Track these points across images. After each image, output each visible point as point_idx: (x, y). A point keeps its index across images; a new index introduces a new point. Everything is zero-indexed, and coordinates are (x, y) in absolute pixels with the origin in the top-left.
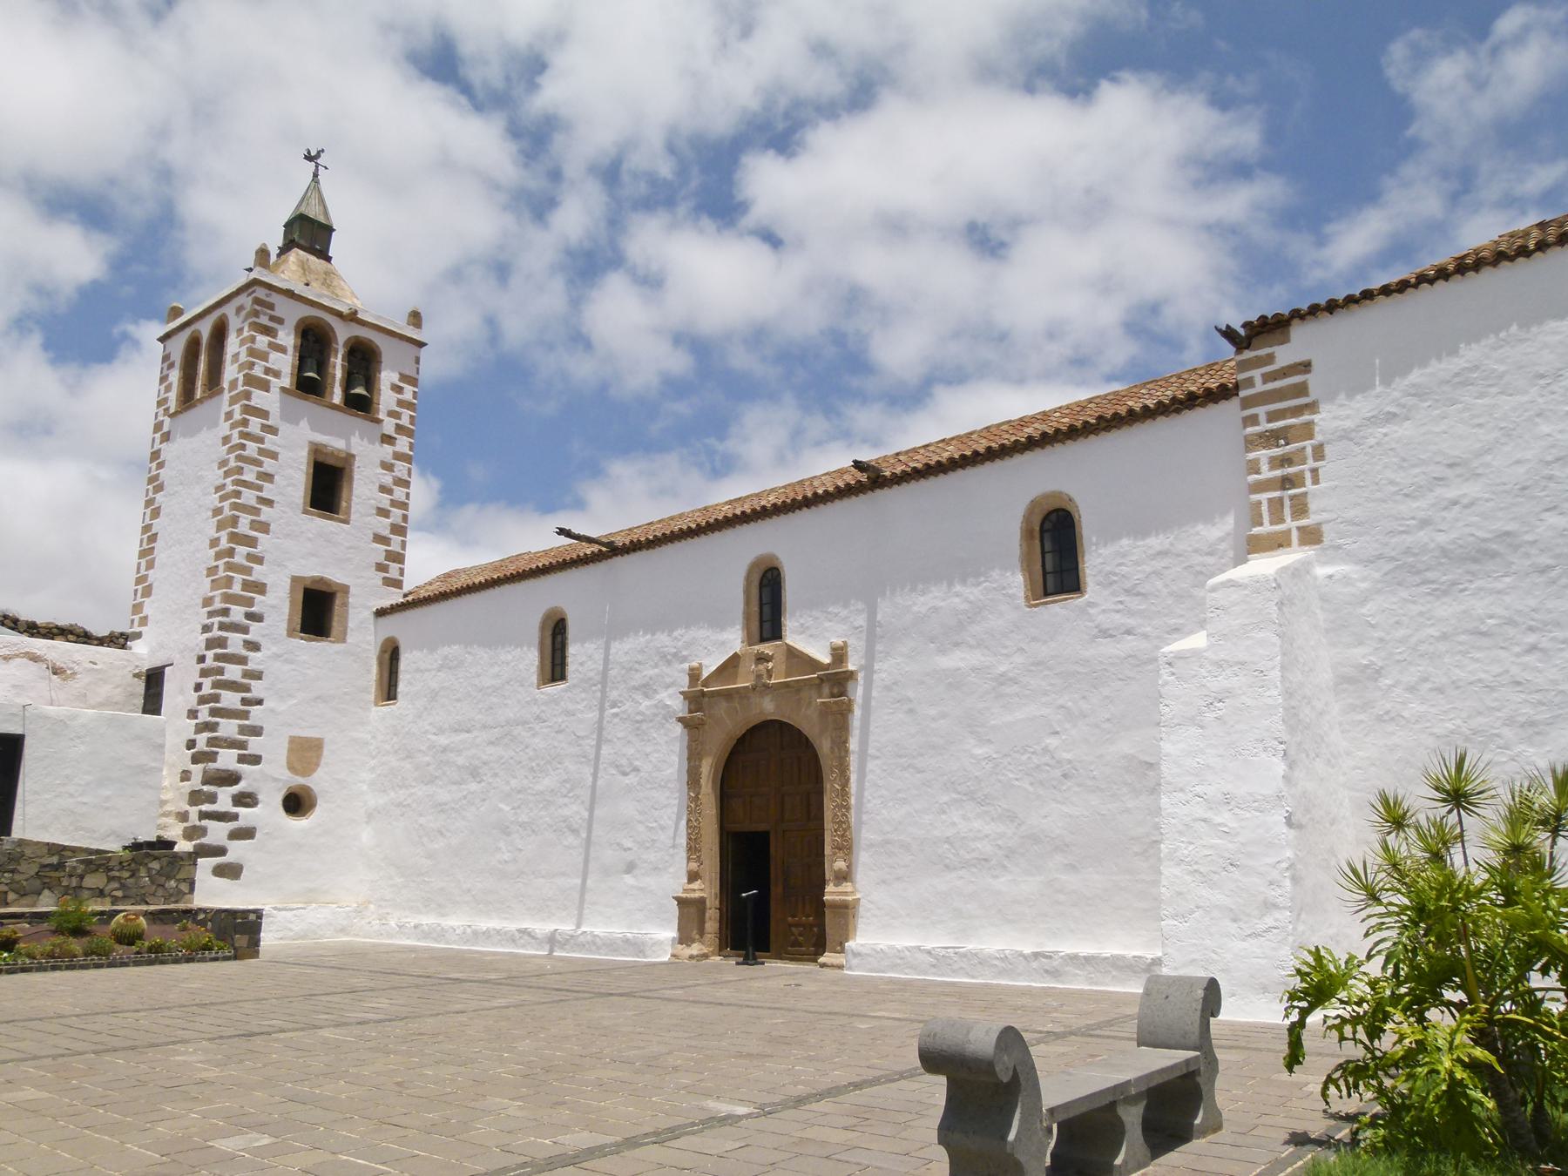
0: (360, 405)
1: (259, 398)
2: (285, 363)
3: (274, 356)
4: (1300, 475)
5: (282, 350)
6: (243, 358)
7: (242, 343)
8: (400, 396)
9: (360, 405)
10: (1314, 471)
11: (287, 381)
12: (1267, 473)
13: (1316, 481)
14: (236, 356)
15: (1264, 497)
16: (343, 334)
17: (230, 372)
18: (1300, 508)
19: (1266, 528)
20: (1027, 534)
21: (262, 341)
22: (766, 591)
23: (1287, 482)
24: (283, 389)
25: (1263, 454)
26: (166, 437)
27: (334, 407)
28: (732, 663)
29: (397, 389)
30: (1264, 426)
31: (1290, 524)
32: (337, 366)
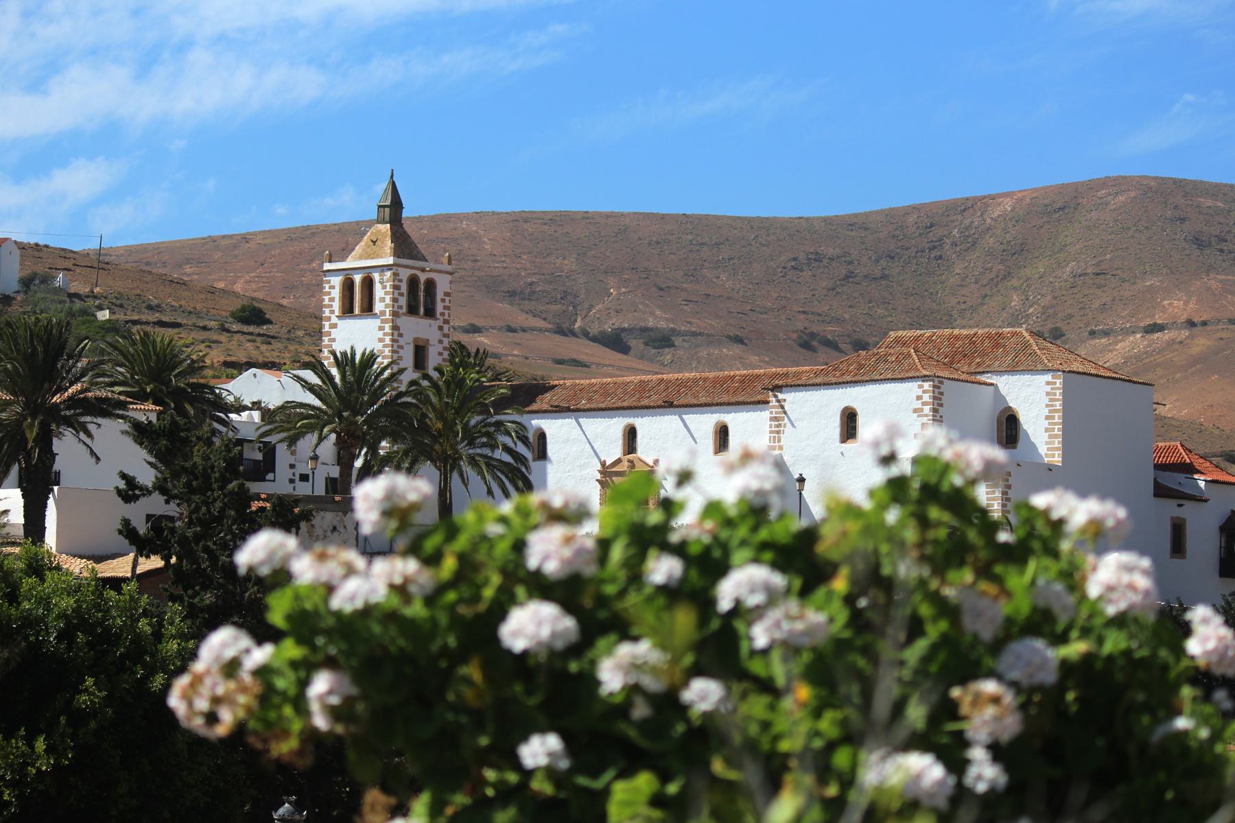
0: (430, 313)
1: (399, 322)
2: (403, 301)
3: (400, 298)
4: (780, 431)
5: (401, 294)
6: (388, 300)
7: (386, 293)
8: (445, 304)
9: (430, 313)
10: (783, 430)
11: (404, 310)
12: (773, 429)
13: (783, 434)
14: (382, 300)
15: (772, 435)
16: (423, 277)
17: (378, 307)
18: (779, 441)
19: (772, 444)
20: (716, 432)
21: (396, 292)
22: (631, 436)
23: (778, 432)
24: (403, 314)
25: (773, 423)
26: (334, 326)
27: (421, 318)
28: (619, 461)
29: (443, 300)
30: (774, 415)
31: (776, 444)
32: (422, 294)
